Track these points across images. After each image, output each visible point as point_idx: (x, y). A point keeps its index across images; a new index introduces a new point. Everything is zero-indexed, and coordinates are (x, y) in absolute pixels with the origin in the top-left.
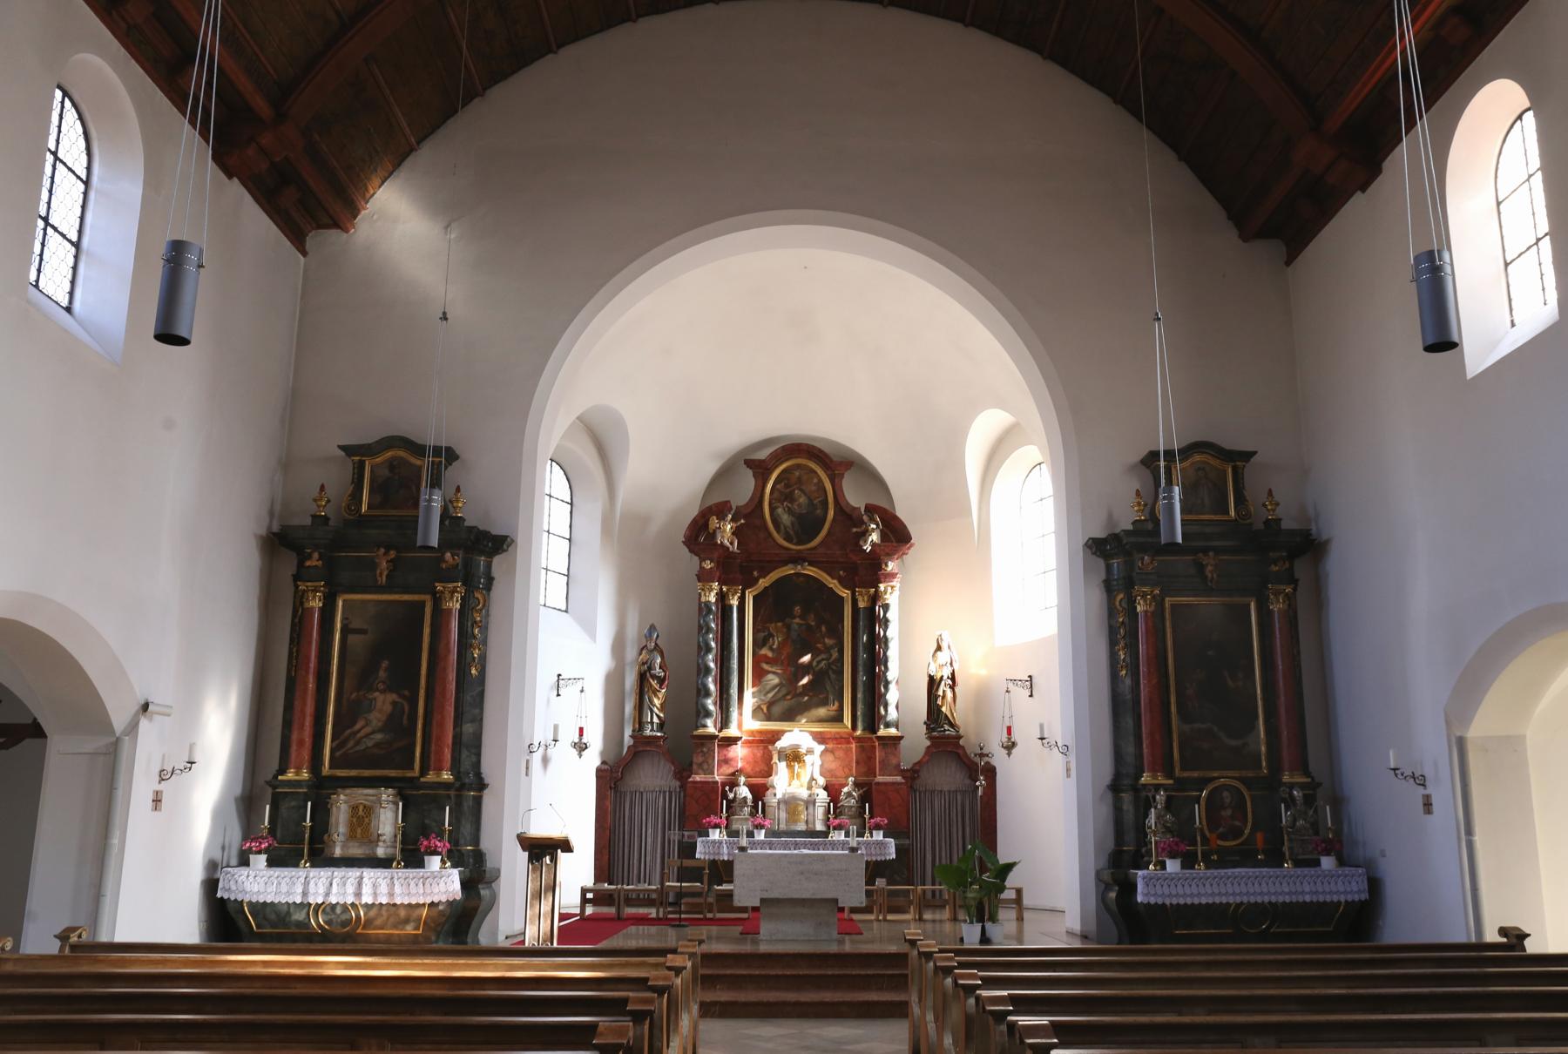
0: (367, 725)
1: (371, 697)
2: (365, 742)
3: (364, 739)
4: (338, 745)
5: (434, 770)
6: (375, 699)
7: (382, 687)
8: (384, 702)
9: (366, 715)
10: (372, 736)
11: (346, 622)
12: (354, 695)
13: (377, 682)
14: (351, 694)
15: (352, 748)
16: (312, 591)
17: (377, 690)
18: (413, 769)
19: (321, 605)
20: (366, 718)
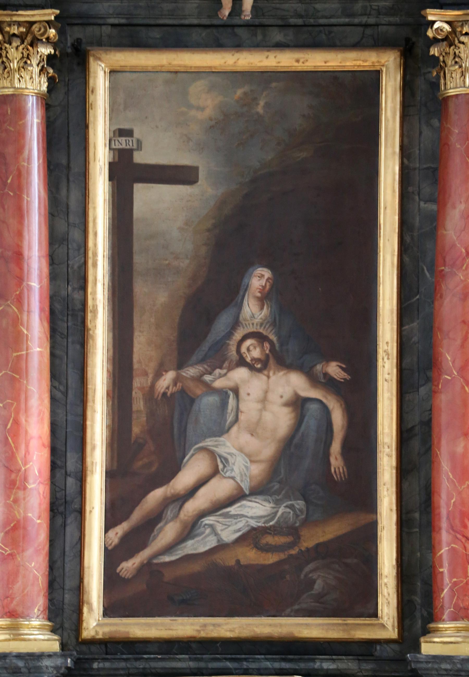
0: (215, 472)
1: (218, 384)
2: (214, 532)
3: (208, 520)
4: (125, 538)
5: (454, 618)
6: (236, 391)
7: (256, 353)
8: (264, 400)
9: (209, 442)
10: (232, 510)
11: (123, 143)
12: (170, 376)
13: (238, 336)
14: (158, 375)
15: (169, 549)
16: (22, 37)
17: (242, 362)
18: (375, 615)
19: (44, 87)
20: (213, 455)
